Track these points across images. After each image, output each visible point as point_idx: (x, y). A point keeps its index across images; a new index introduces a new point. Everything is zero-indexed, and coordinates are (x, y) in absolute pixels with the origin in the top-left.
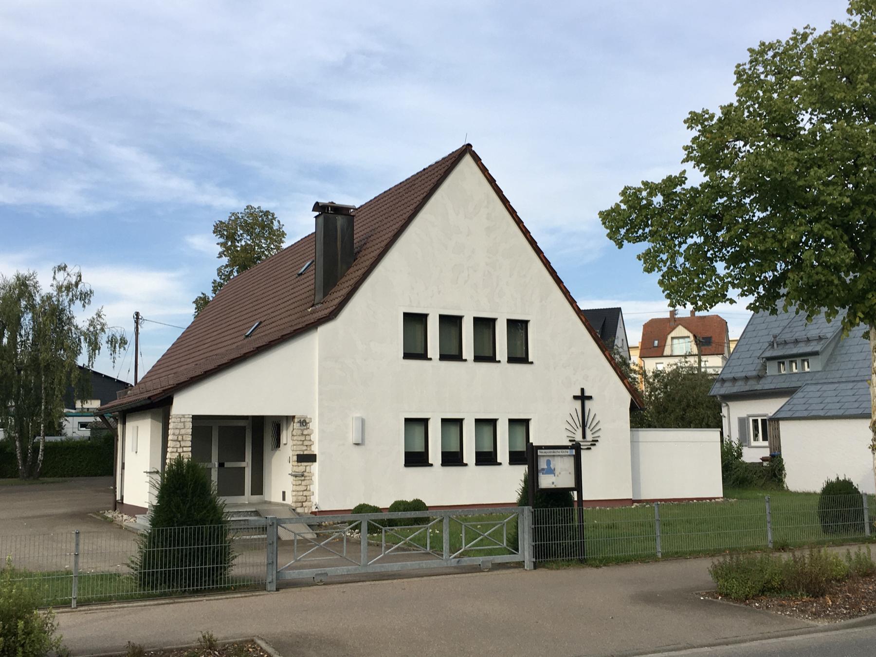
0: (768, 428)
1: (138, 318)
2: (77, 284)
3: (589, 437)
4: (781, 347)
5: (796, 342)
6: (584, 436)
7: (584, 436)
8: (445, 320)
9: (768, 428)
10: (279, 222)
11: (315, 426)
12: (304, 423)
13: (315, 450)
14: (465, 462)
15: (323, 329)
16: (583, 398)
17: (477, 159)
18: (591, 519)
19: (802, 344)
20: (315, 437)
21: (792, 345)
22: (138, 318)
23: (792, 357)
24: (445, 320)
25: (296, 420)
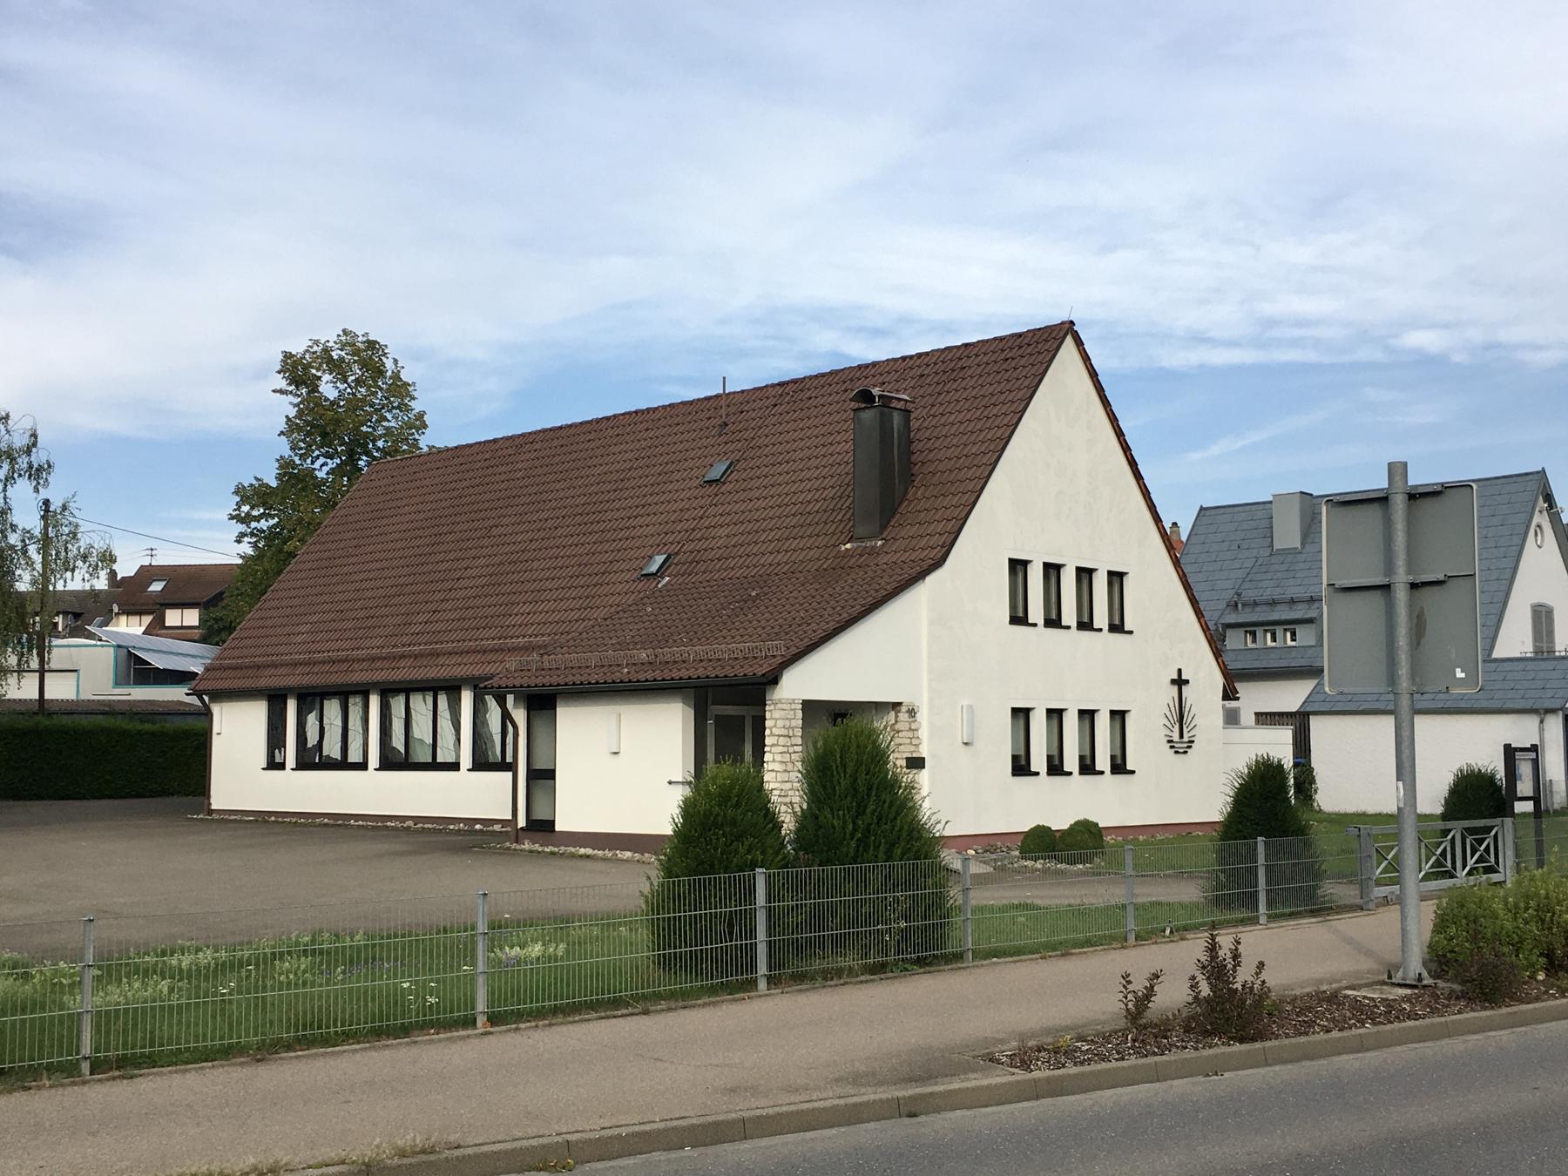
0: (1299, 722)
1: (47, 511)
2: (28, 452)
3: (1186, 739)
4: (1247, 609)
5: (1273, 603)
6: (1181, 736)
7: (1181, 736)
8: (1048, 567)
9: (1299, 722)
10: (396, 361)
11: (923, 717)
12: (912, 712)
13: (924, 751)
14: (1066, 769)
15: (931, 579)
16: (1180, 682)
17: (1079, 343)
18: (1324, 841)
19: (1301, 606)
20: (924, 733)
21: (1305, 606)
22: (47, 511)
23: (1270, 625)
24: (1048, 567)
25: (904, 709)
